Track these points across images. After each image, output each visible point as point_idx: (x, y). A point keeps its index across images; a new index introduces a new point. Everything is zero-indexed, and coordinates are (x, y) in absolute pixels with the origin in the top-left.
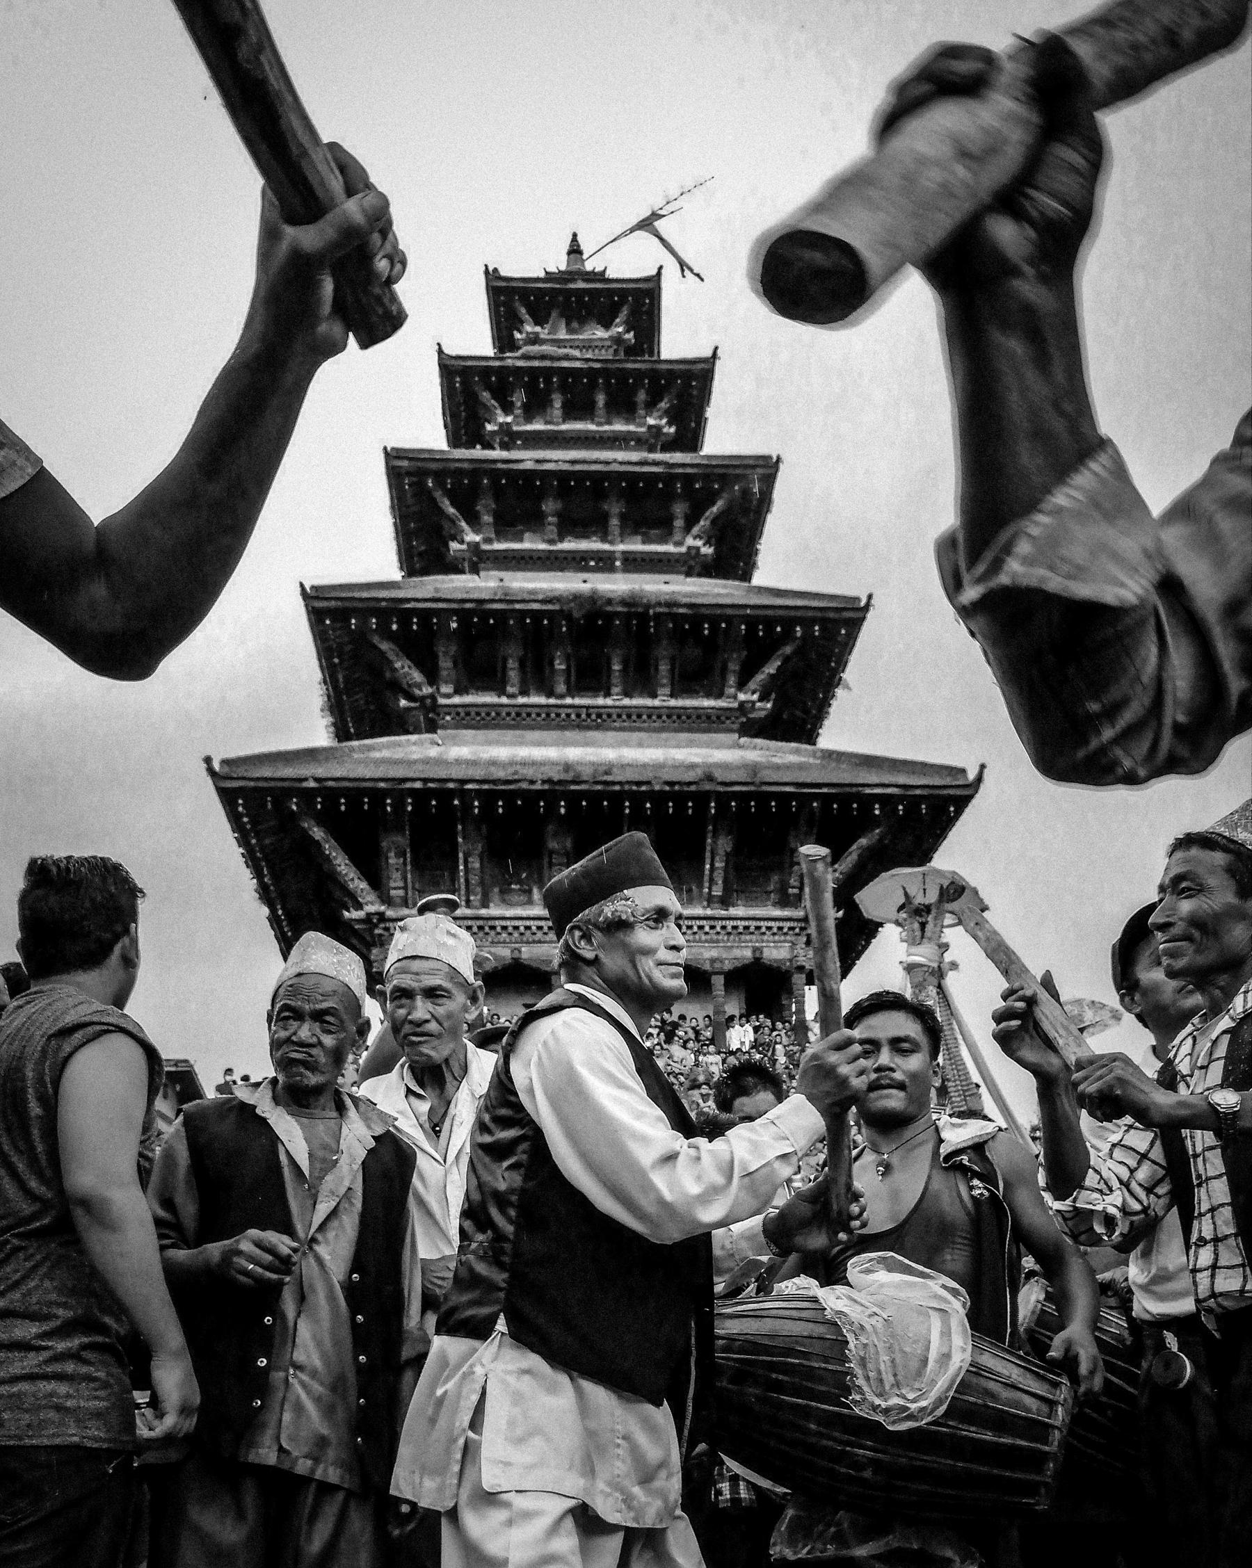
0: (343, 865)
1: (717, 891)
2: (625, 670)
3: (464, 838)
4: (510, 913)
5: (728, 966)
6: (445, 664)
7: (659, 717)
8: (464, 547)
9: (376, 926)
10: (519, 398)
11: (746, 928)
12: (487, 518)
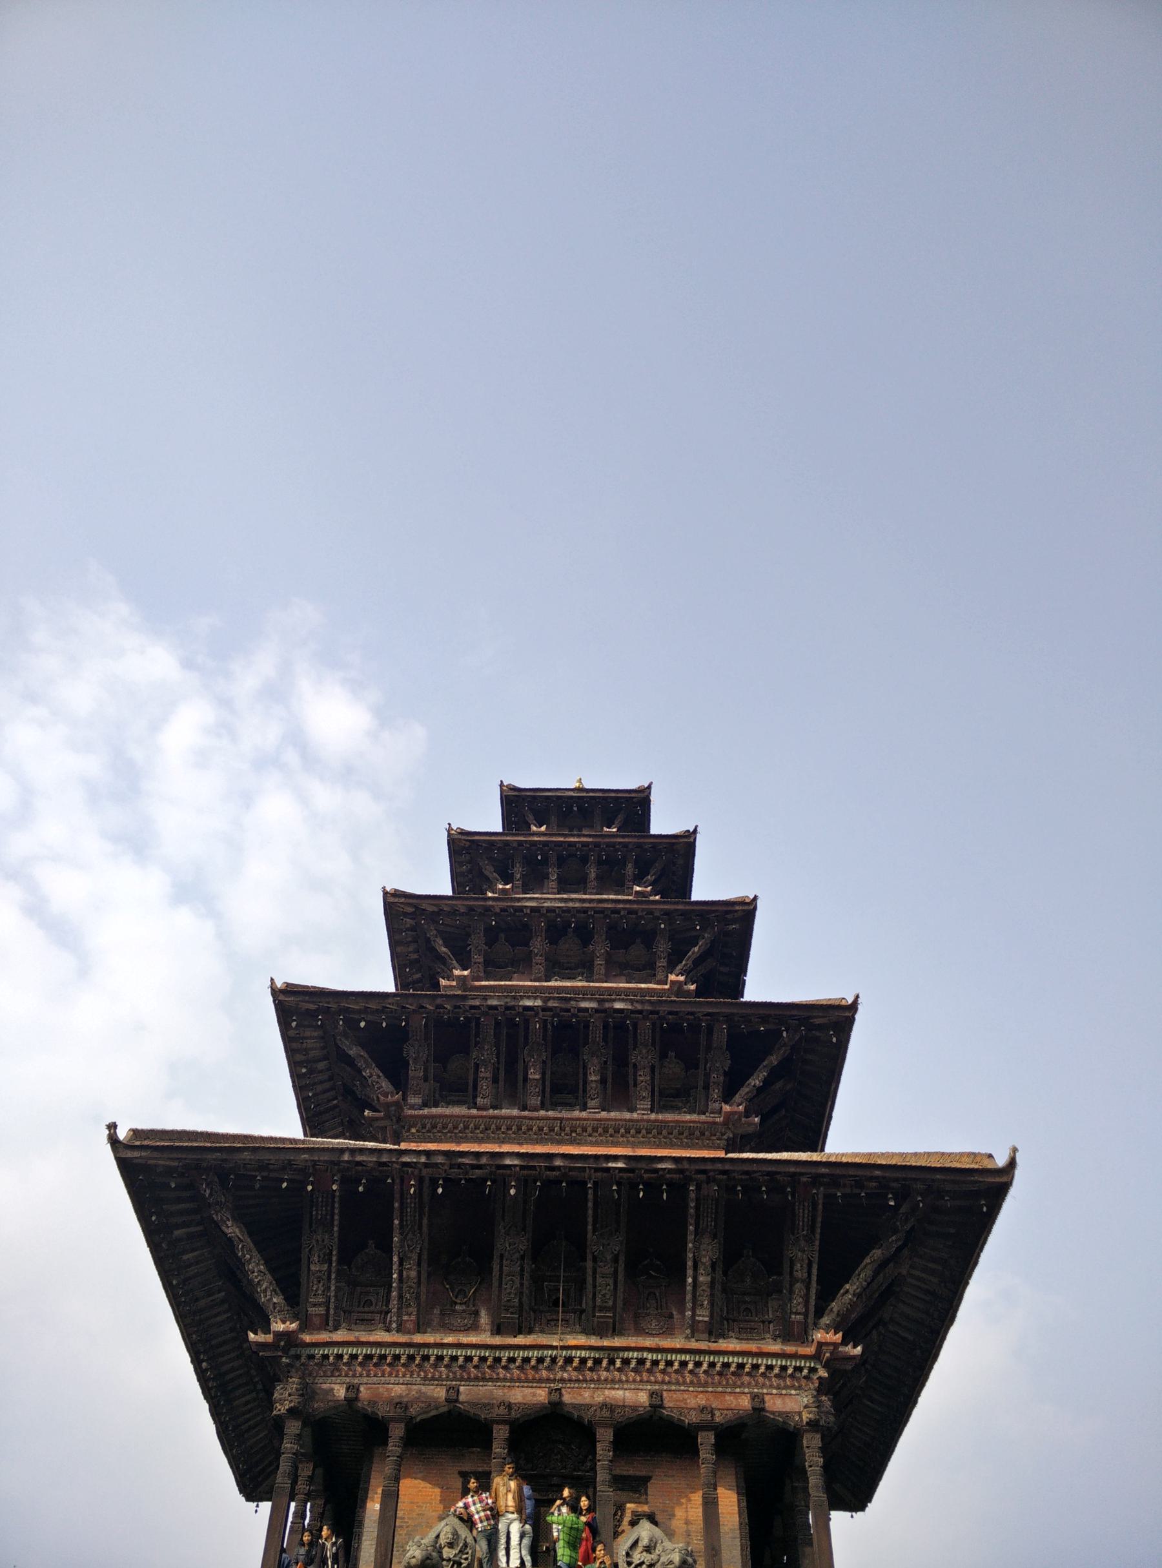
0: (256, 1270)
1: (703, 1316)
2: (603, 1081)
3: (401, 1234)
4: (449, 1339)
5: (718, 1418)
6: (415, 1072)
7: (638, 1132)
8: (454, 983)
9: (285, 1350)
10: (518, 871)
11: (741, 1366)
12: (477, 958)
